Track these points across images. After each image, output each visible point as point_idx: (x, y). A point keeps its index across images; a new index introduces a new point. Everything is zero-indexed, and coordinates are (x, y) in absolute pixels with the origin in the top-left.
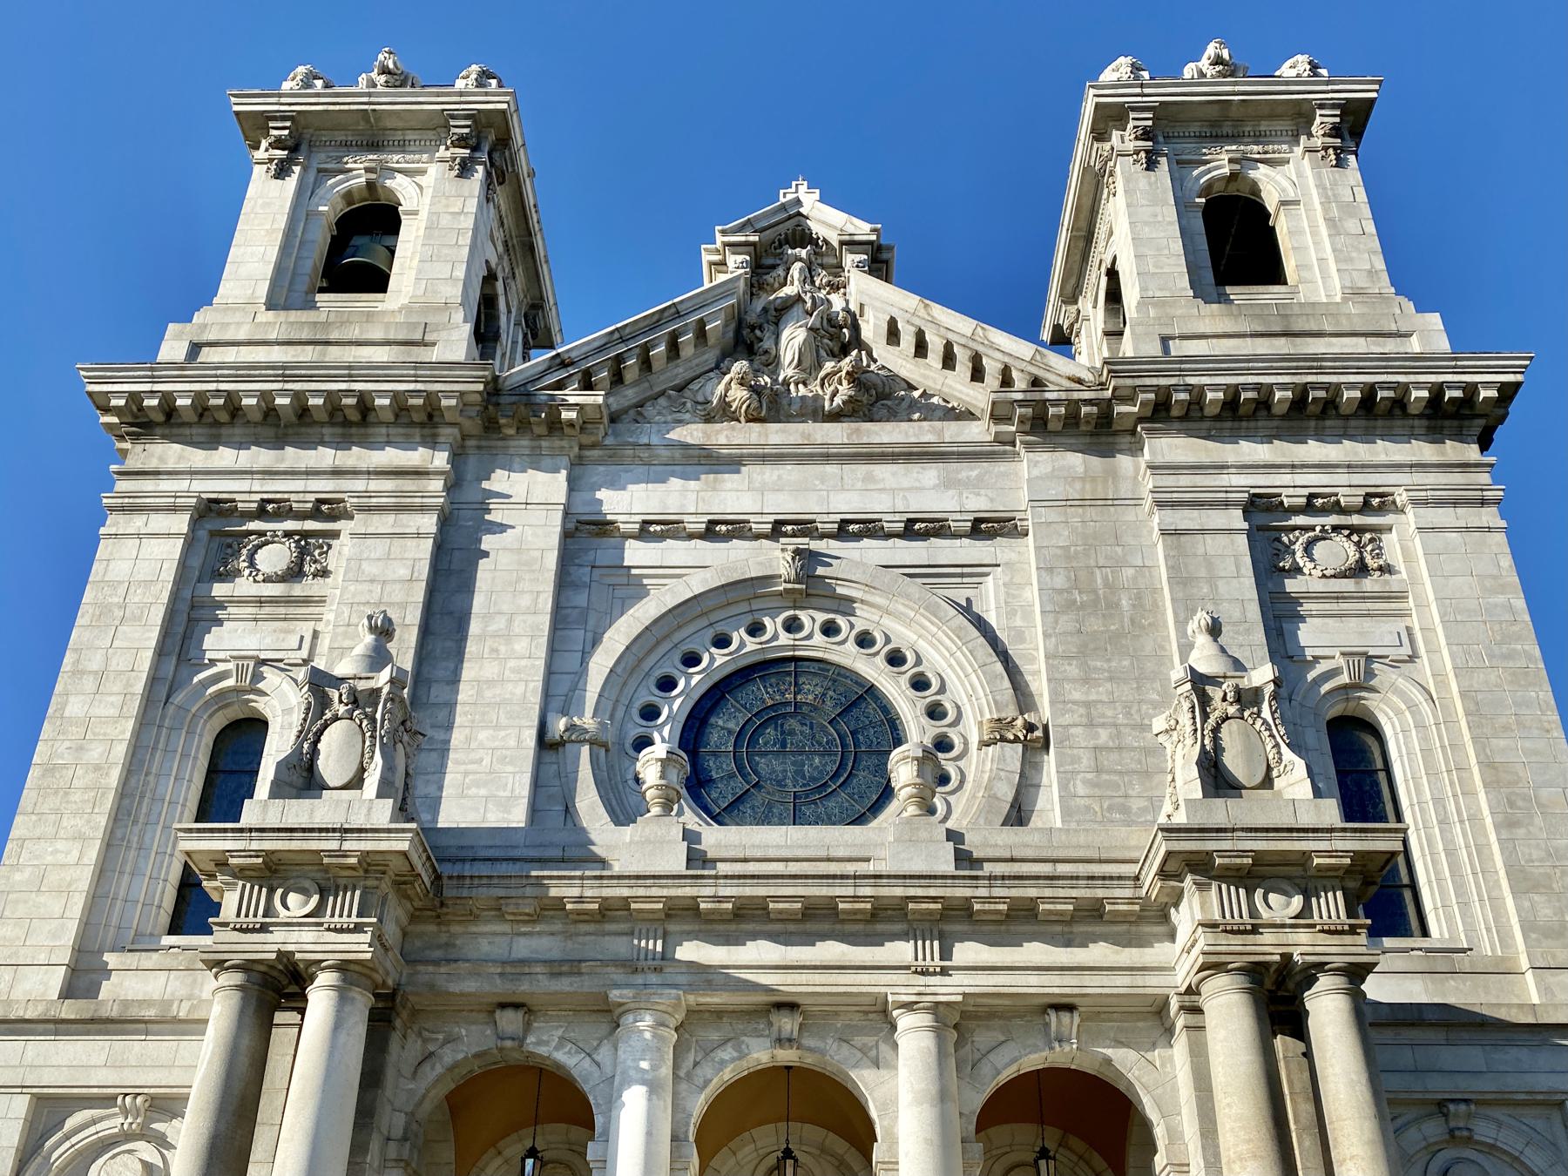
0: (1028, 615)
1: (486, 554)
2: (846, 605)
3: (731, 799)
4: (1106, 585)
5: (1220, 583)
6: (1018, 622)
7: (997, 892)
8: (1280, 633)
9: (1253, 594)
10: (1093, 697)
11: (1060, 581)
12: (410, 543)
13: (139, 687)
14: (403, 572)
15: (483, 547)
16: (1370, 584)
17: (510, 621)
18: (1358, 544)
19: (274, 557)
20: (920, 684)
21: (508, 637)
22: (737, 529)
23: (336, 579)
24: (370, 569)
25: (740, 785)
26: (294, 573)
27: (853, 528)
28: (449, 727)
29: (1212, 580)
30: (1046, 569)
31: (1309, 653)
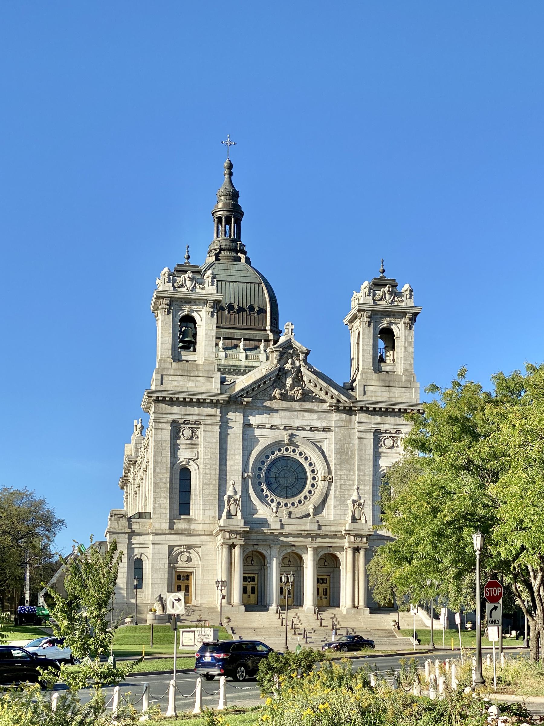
0: (332, 452)
1: (229, 434)
2: (298, 446)
3: (275, 487)
4: (347, 448)
5: (367, 451)
6: (330, 453)
7: (323, 533)
8: (376, 460)
9: (372, 454)
10: (341, 473)
11: (338, 447)
12: (215, 433)
13: (169, 466)
14: (214, 441)
15: (228, 432)
16: (393, 450)
17: (235, 451)
18: (394, 441)
19: (187, 433)
20: (311, 464)
21: (235, 455)
22: (277, 427)
23: (201, 440)
24: (208, 439)
25: (276, 485)
26: (191, 438)
27: (300, 428)
28: (226, 475)
29: (365, 450)
30: (336, 443)
31: (380, 465)
